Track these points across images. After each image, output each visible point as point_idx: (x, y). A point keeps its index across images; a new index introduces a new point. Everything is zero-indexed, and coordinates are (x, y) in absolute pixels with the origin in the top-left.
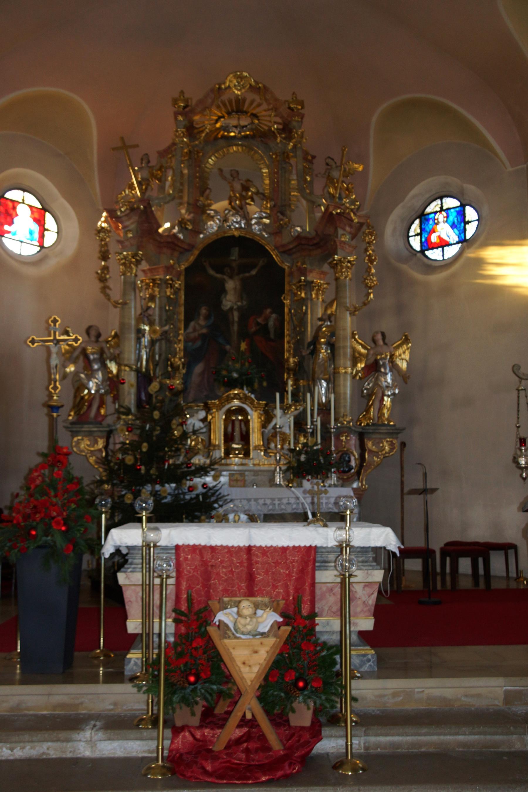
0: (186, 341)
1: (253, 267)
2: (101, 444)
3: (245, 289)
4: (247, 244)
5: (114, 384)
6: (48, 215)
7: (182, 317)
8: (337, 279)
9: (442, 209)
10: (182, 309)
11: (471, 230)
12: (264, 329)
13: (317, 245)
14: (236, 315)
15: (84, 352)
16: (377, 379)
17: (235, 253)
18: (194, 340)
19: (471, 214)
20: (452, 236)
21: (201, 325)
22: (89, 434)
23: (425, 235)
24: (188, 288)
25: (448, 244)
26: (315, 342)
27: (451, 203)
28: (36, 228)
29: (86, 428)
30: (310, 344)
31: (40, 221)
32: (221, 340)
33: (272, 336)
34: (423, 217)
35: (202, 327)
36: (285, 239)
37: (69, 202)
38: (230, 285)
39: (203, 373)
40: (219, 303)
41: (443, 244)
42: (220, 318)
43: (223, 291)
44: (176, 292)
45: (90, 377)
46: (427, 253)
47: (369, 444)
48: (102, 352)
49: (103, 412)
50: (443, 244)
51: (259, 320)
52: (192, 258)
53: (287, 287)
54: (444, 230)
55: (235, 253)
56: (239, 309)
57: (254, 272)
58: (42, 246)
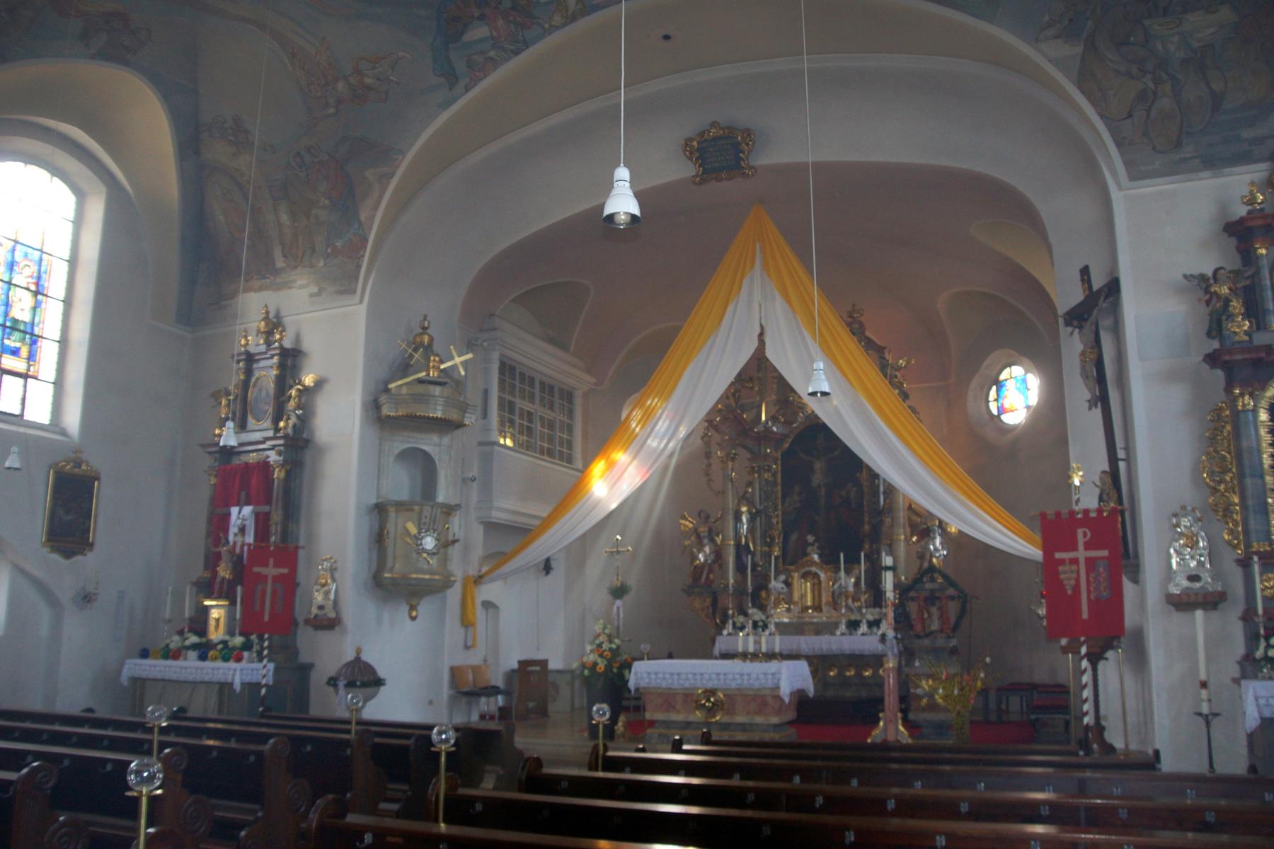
2: (709, 601)
5: (718, 554)
7: (780, 494)
10: (779, 488)
14: (823, 491)
24: (784, 469)
29: (696, 590)
38: (818, 466)
44: (774, 475)
45: (700, 550)
48: (710, 530)
49: (711, 576)
51: (843, 493)
52: (786, 445)
57: (836, 453)
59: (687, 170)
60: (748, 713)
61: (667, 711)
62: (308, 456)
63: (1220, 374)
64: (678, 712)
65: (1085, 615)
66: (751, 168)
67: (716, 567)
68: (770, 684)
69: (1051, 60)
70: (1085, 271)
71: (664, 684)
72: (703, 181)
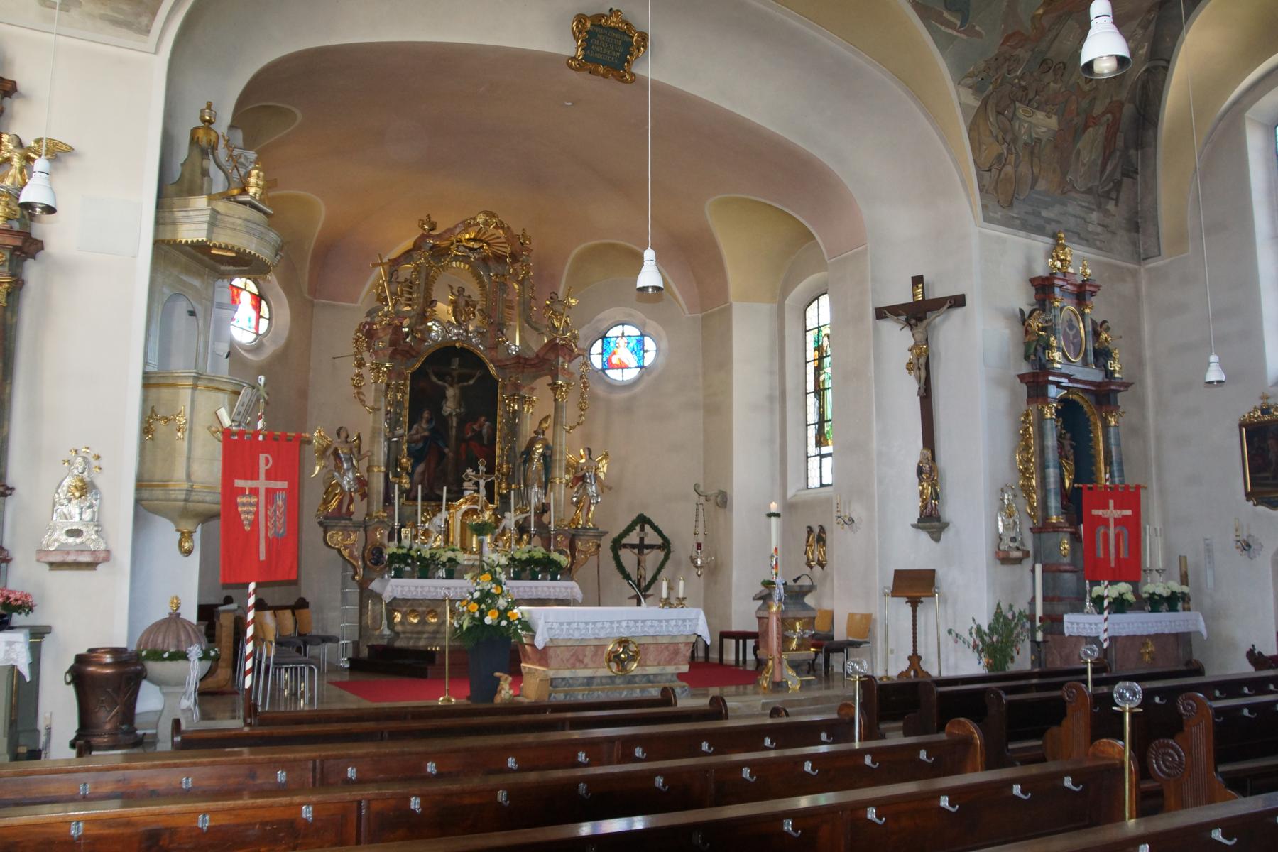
0: (409, 442)
1: (471, 377)
3: (464, 397)
4: (466, 356)
6: (263, 303)
7: (406, 420)
8: (556, 400)
9: (623, 335)
11: (649, 359)
12: (479, 434)
13: (533, 366)
14: (455, 420)
15: (336, 450)
16: (585, 489)
17: (456, 361)
18: (416, 442)
19: (649, 344)
20: (632, 361)
21: (423, 428)
22: (345, 528)
23: (606, 355)
25: (627, 367)
26: (529, 451)
27: (631, 331)
28: (253, 314)
30: (523, 453)
31: (257, 308)
32: (441, 443)
33: (485, 442)
34: (603, 337)
35: (425, 430)
36: (500, 355)
37: (284, 289)
38: (450, 392)
39: (423, 473)
40: (441, 408)
41: (622, 367)
42: (441, 422)
43: (444, 397)
46: (608, 372)
47: (579, 544)
50: (622, 367)
52: (417, 365)
53: (499, 398)
54: (623, 354)
55: (456, 361)
56: (457, 415)
57: (471, 382)
58: (257, 334)
59: (569, 48)
60: (659, 664)
61: (574, 667)
62: (32, 271)
63: (1025, 386)
64: (586, 667)
65: (262, 557)
66: (633, 74)
67: (357, 497)
68: (688, 631)
69: (956, 100)
70: (917, 281)
71: (577, 635)
72: (580, 68)
